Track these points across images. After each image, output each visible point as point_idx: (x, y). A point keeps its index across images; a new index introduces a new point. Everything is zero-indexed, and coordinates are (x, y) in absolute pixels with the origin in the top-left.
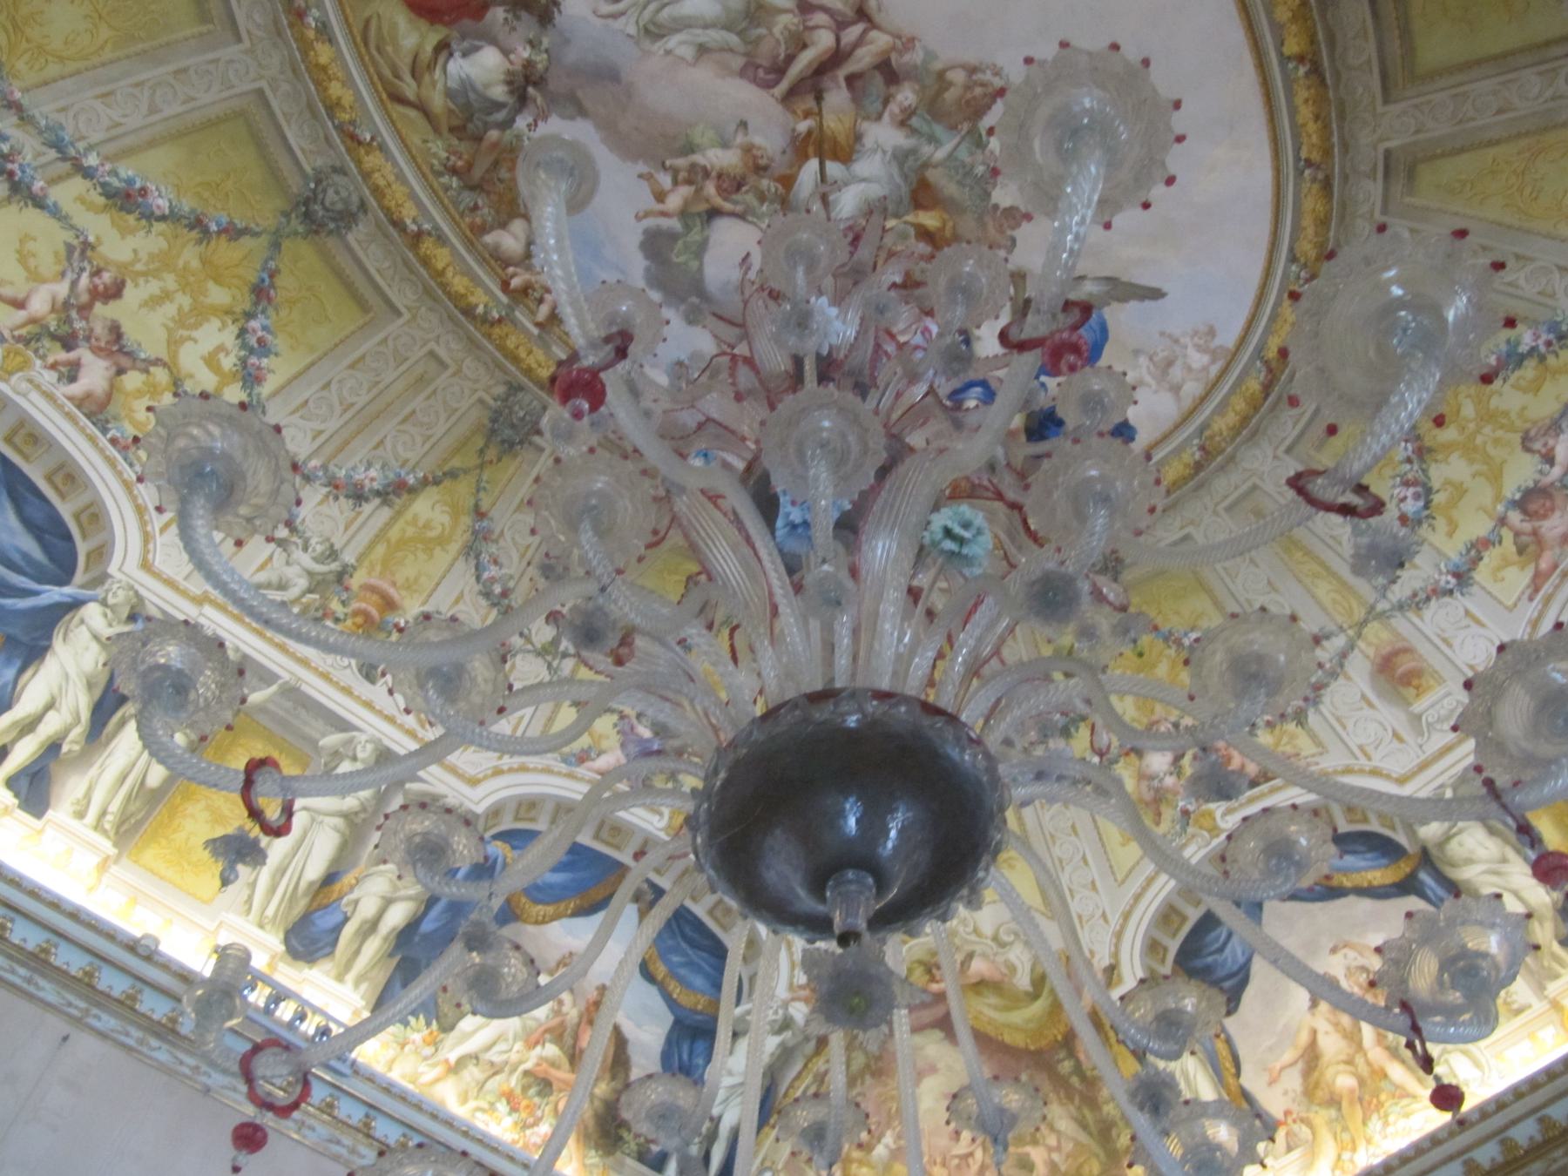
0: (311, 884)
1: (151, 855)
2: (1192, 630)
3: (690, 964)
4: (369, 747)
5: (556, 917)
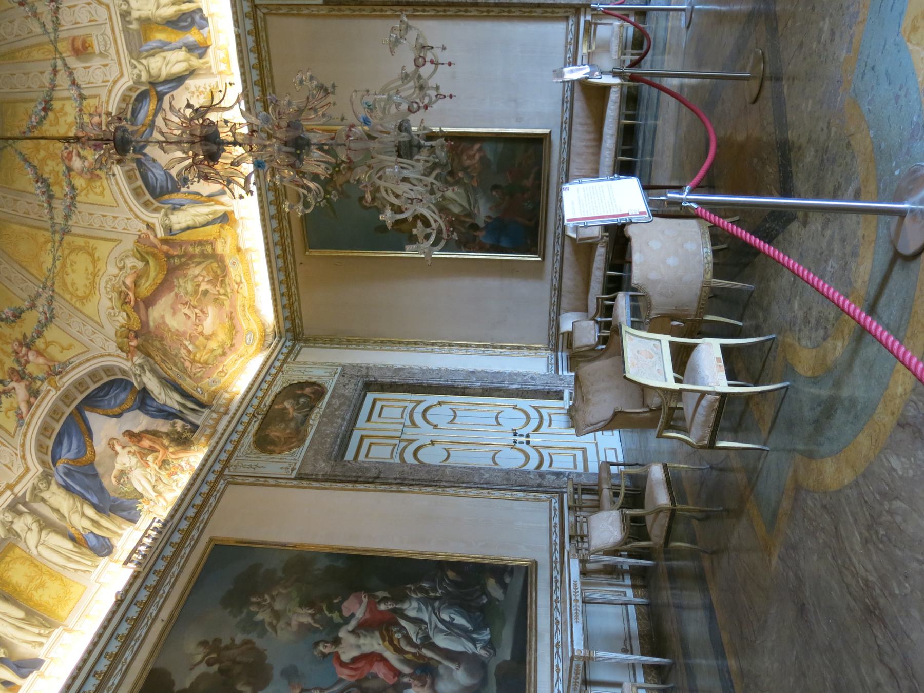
0: (75, 546)
1: (62, 613)
2: (31, 118)
3: (116, 397)
4: (6, 514)
5: (92, 447)
